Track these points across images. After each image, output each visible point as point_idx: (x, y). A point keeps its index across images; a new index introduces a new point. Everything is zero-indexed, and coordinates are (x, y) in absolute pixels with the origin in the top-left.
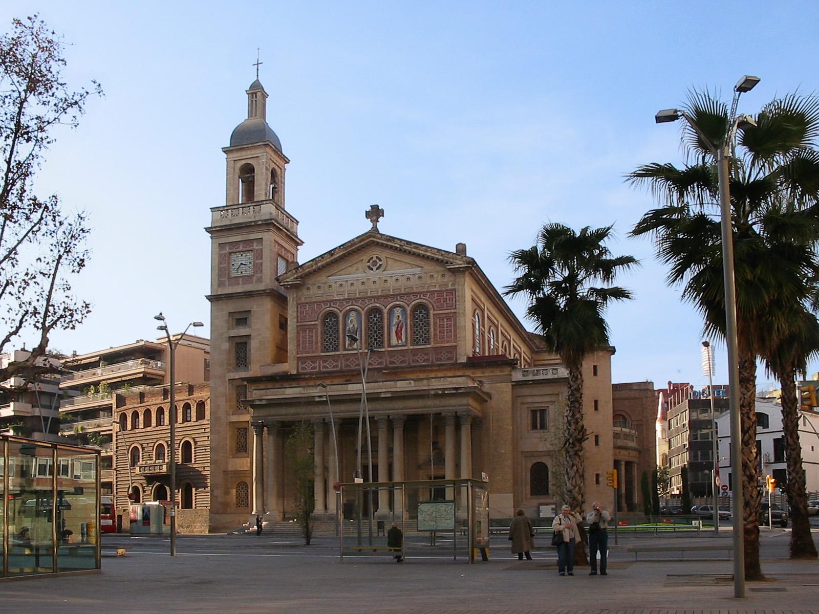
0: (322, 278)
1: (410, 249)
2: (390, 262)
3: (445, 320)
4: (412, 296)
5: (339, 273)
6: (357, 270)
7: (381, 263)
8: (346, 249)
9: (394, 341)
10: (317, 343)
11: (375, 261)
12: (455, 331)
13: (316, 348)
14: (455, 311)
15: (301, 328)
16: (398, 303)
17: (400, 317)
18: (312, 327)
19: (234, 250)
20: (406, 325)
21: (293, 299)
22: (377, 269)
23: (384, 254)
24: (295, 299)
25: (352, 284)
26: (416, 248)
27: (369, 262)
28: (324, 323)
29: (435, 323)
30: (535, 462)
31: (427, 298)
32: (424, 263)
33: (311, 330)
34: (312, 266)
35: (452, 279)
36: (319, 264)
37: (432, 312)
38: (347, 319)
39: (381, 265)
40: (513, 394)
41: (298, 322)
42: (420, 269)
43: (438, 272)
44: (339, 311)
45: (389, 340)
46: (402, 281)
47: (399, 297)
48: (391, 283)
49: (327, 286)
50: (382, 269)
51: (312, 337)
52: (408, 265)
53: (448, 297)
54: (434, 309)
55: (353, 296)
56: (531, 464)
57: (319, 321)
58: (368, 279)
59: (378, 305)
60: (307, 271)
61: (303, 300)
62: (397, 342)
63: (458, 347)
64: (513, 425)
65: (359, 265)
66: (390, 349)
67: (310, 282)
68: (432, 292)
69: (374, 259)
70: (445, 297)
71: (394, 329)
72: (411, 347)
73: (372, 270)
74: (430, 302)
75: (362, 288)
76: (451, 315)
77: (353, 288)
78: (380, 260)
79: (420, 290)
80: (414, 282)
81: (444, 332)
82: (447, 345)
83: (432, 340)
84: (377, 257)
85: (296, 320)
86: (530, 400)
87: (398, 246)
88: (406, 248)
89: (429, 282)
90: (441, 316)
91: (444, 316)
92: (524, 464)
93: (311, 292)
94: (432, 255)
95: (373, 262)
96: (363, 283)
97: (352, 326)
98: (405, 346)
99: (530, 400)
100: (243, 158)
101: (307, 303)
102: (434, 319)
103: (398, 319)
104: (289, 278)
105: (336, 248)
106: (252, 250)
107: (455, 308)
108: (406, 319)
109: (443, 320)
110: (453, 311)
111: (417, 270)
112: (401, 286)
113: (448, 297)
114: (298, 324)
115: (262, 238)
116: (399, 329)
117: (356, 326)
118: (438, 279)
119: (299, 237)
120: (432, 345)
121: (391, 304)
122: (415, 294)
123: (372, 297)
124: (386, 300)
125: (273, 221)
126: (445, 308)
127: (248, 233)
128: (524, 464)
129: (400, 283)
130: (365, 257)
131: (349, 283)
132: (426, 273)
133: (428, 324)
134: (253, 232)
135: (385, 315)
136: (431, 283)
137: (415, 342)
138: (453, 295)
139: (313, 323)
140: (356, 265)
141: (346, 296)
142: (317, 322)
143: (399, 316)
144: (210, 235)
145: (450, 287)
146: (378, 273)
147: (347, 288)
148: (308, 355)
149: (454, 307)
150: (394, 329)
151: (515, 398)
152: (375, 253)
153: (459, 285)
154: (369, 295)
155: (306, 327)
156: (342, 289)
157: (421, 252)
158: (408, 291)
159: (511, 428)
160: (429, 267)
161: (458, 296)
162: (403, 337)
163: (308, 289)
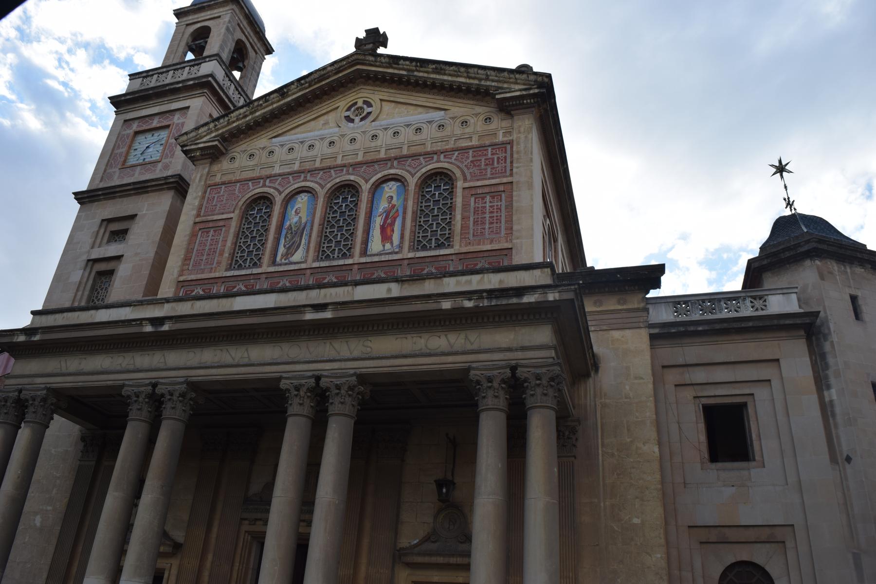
0: (261, 142)
1: (426, 75)
2: (387, 107)
3: (488, 199)
4: (421, 158)
5: (293, 132)
6: (324, 124)
7: (370, 110)
8: (310, 86)
9: (376, 244)
10: (221, 254)
11: (361, 108)
12: (510, 221)
13: (219, 263)
14: (509, 179)
15: (202, 226)
16: (392, 171)
17: (394, 201)
18: (221, 223)
19: (145, 127)
20: (405, 213)
21: (201, 177)
22: (362, 119)
23: (375, 95)
24: (204, 178)
25: (311, 146)
26: (436, 71)
27: (349, 109)
28: (245, 215)
29: (465, 206)
30: (730, 560)
31: (453, 160)
32: (450, 103)
33: (217, 229)
34: (245, 116)
35: (506, 124)
36: (258, 114)
37: (460, 184)
38: (289, 207)
39: (369, 113)
40: (653, 358)
41: (198, 215)
42: (443, 112)
43: (476, 115)
44: (277, 193)
45: (366, 242)
46: (407, 135)
47: (395, 163)
48: (385, 139)
49: (265, 153)
50: (371, 118)
51: (217, 242)
52: (420, 110)
53: (496, 157)
54: (465, 180)
55: (308, 166)
56: (720, 569)
57: (237, 212)
58: (343, 136)
59: (352, 178)
60: (234, 125)
61: (218, 179)
62: (381, 248)
63: (514, 251)
64: (660, 444)
65: (331, 117)
66: (363, 260)
67: (238, 149)
68: (467, 149)
69: (360, 103)
70: (490, 156)
71: (378, 221)
72: (411, 255)
73: (352, 121)
74: (458, 167)
75: (329, 151)
76: (501, 188)
77: (311, 153)
78: (369, 105)
79: (439, 147)
80: (429, 133)
81: (484, 223)
82: (489, 247)
83: (457, 238)
84: (365, 102)
85: (194, 212)
86: (700, 376)
87: (404, 73)
88: (421, 74)
89: (458, 131)
90: (479, 191)
91: (486, 190)
92: (698, 564)
93: (236, 164)
94: (468, 81)
95: (357, 109)
96: (332, 143)
97: (296, 219)
98: (396, 253)
99: (700, 376)
100: (200, 19)
101: (223, 183)
102: (463, 198)
103: (390, 203)
104: (201, 138)
105: (292, 83)
106: (168, 126)
107: (511, 175)
108: (406, 200)
109: (483, 198)
110: (505, 180)
111: (437, 115)
112: (403, 143)
113: (496, 157)
114: (198, 220)
115: (188, 108)
116: (389, 221)
117: (304, 220)
118: (477, 125)
119: (224, 72)
120: (458, 247)
121: (379, 175)
122: (429, 155)
123: (344, 166)
124: (371, 169)
125: (210, 79)
126: (489, 176)
127: (171, 101)
128: (698, 564)
129: (401, 138)
130: (342, 102)
131: (307, 145)
132: (453, 118)
133: (451, 208)
134: (178, 100)
135: (365, 197)
136: (464, 134)
137: (418, 244)
138: (506, 152)
139: (224, 216)
140: (325, 117)
141: (296, 167)
142: (231, 215)
143: (392, 197)
144: (116, 110)
145: (501, 138)
146: (363, 126)
147: (302, 152)
148: (199, 276)
149: (508, 173)
150: (378, 221)
151: (660, 370)
152: (361, 94)
153: (520, 132)
154: (339, 161)
155: (211, 225)
156: (290, 157)
157: (446, 78)
158: (414, 150)
159: (656, 449)
160: (459, 109)
161: (518, 152)
162: (396, 238)
163: (233, 159)
